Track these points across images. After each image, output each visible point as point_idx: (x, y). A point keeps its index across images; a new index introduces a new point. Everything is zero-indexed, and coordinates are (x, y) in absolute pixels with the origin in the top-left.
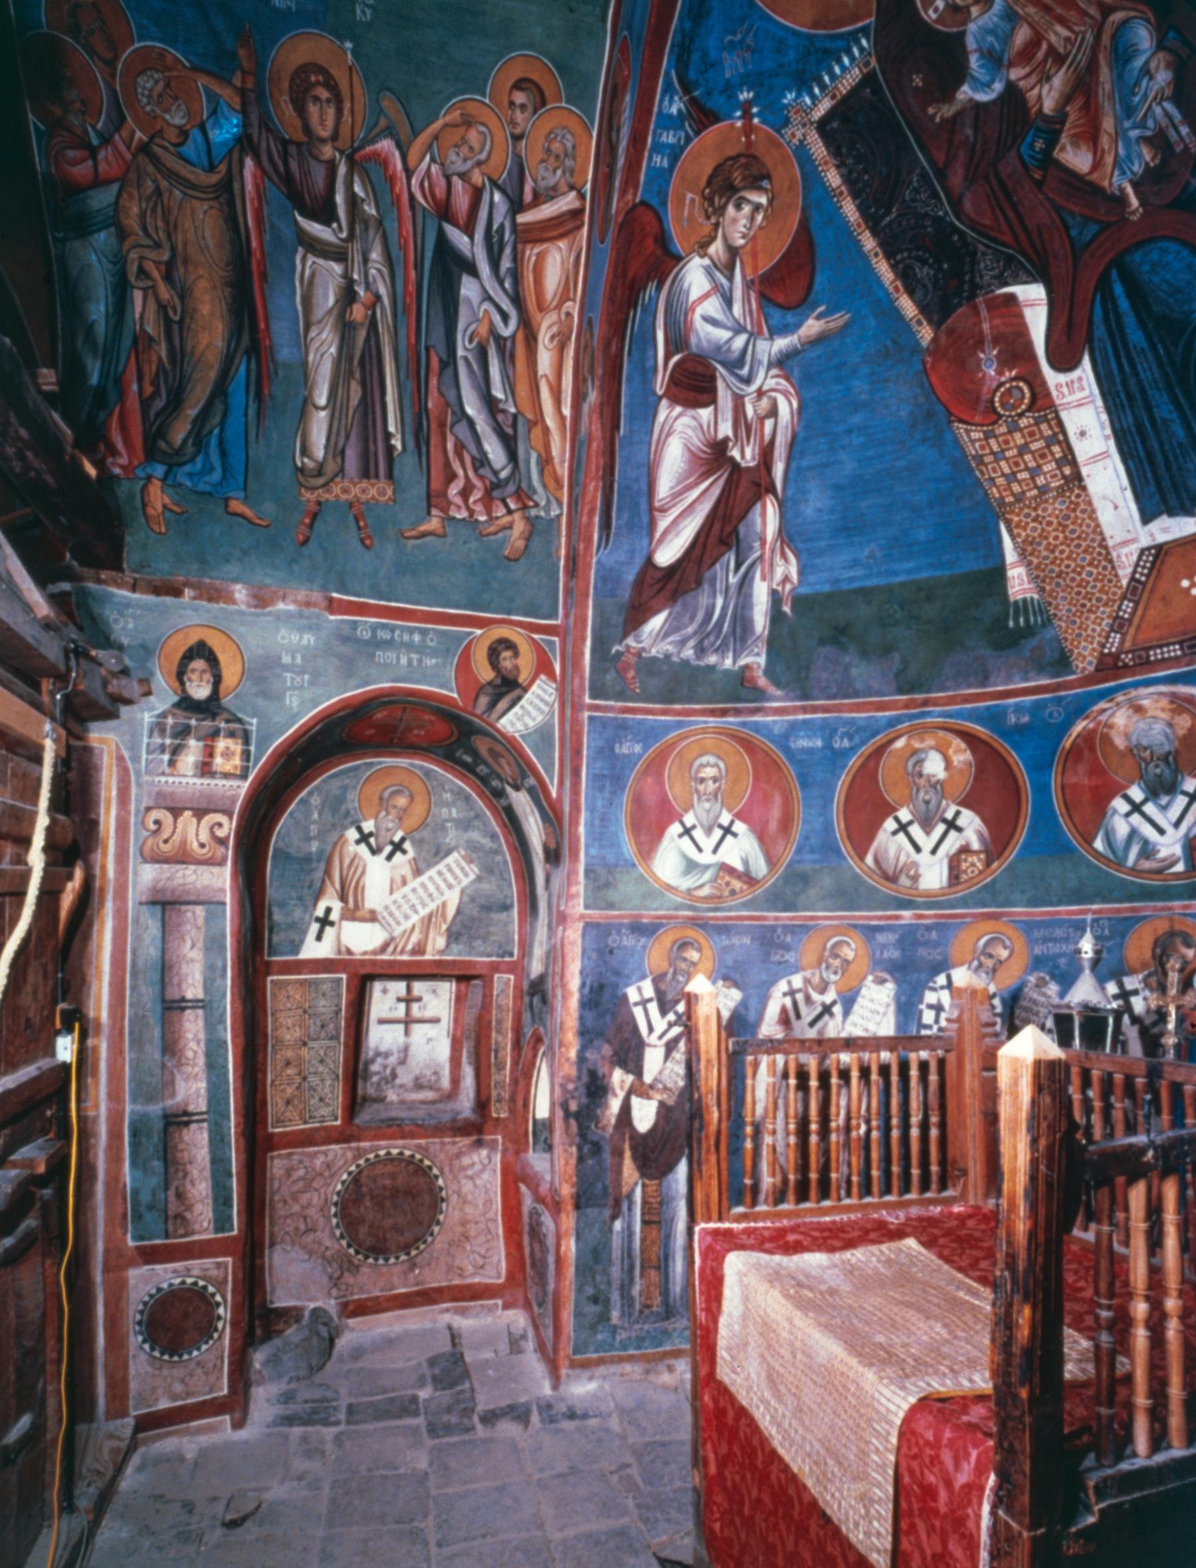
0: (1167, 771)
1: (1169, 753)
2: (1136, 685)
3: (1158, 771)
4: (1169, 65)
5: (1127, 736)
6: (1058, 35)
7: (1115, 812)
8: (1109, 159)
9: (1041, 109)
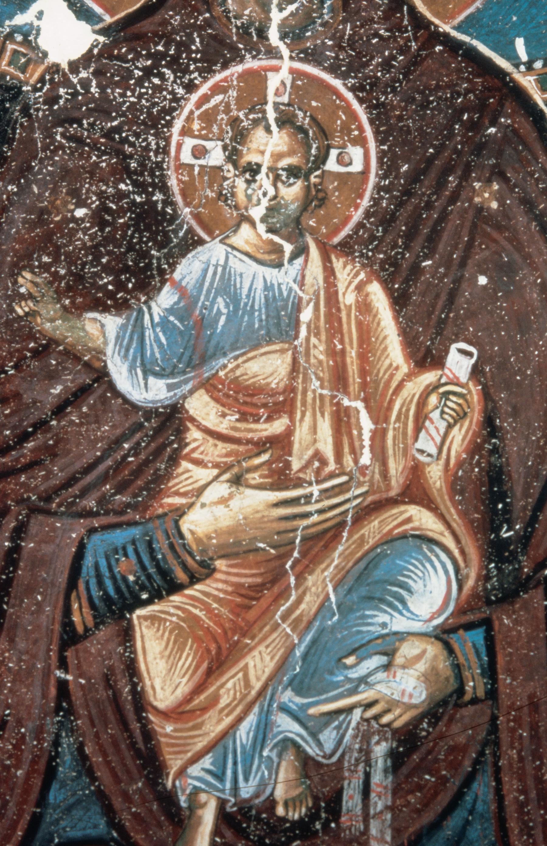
4: (428, 678)
6: (312, 434)
8: (213, 726)
9: (180, 512)
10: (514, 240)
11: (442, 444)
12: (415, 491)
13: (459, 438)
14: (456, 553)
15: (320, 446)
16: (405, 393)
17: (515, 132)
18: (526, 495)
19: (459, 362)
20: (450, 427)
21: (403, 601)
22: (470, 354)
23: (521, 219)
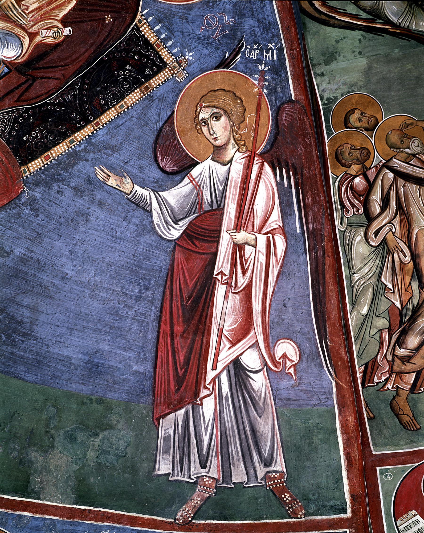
10: (101, 30)
11: (46, 37)
12: (32, 36)
13: (50, 40)
14: (23, 54)
15: (31, 6)
16: (54, 21)
17: (126, 19)
18: (46, 63)
19: (67, 31)
20: (51, 36)
21: (4, 47)
22: (70, 33)
23: (107, 30)
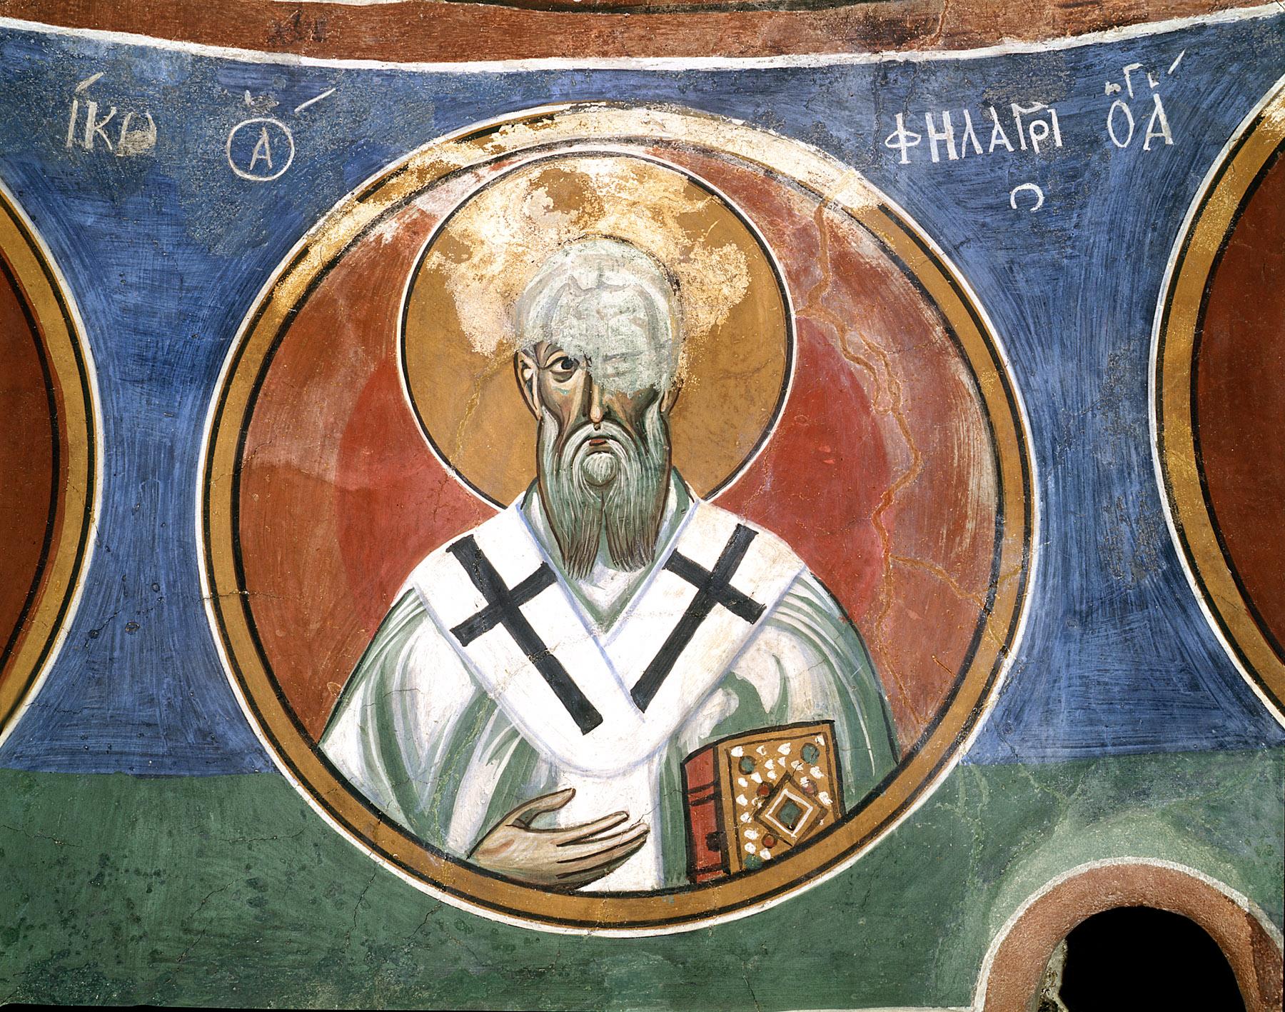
0: (632, 469)
1: (652, 395)
2: (588, 92)
3: (599, 464)
5: (510, 300)
7: (423, 611)
